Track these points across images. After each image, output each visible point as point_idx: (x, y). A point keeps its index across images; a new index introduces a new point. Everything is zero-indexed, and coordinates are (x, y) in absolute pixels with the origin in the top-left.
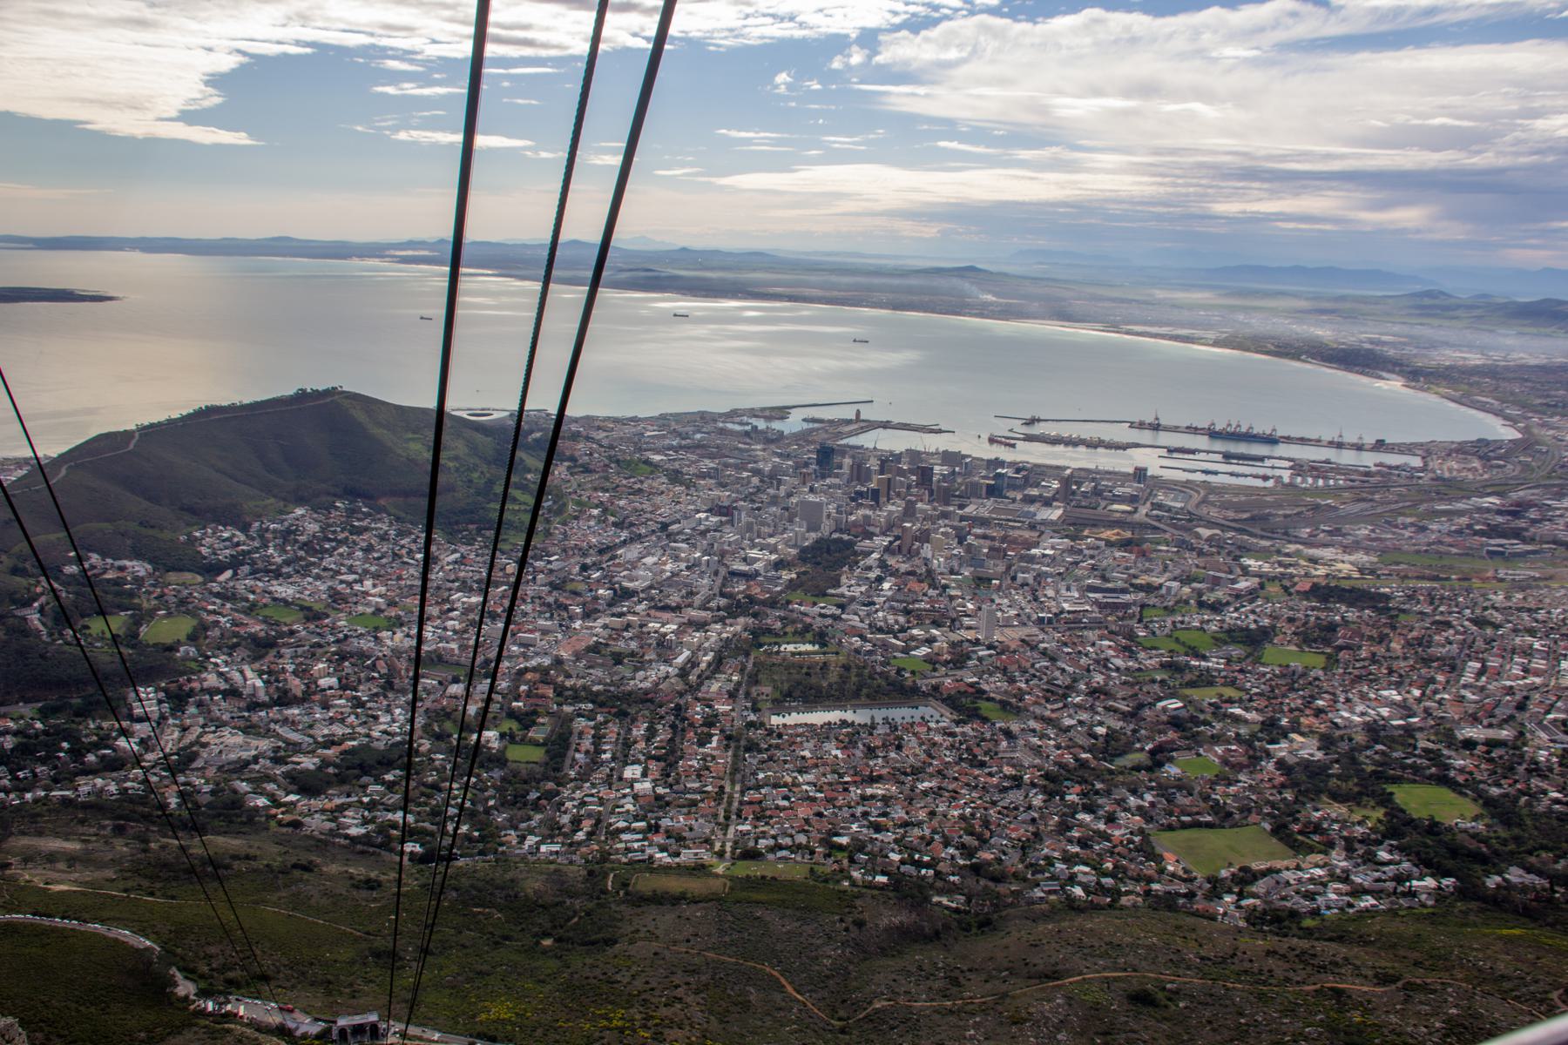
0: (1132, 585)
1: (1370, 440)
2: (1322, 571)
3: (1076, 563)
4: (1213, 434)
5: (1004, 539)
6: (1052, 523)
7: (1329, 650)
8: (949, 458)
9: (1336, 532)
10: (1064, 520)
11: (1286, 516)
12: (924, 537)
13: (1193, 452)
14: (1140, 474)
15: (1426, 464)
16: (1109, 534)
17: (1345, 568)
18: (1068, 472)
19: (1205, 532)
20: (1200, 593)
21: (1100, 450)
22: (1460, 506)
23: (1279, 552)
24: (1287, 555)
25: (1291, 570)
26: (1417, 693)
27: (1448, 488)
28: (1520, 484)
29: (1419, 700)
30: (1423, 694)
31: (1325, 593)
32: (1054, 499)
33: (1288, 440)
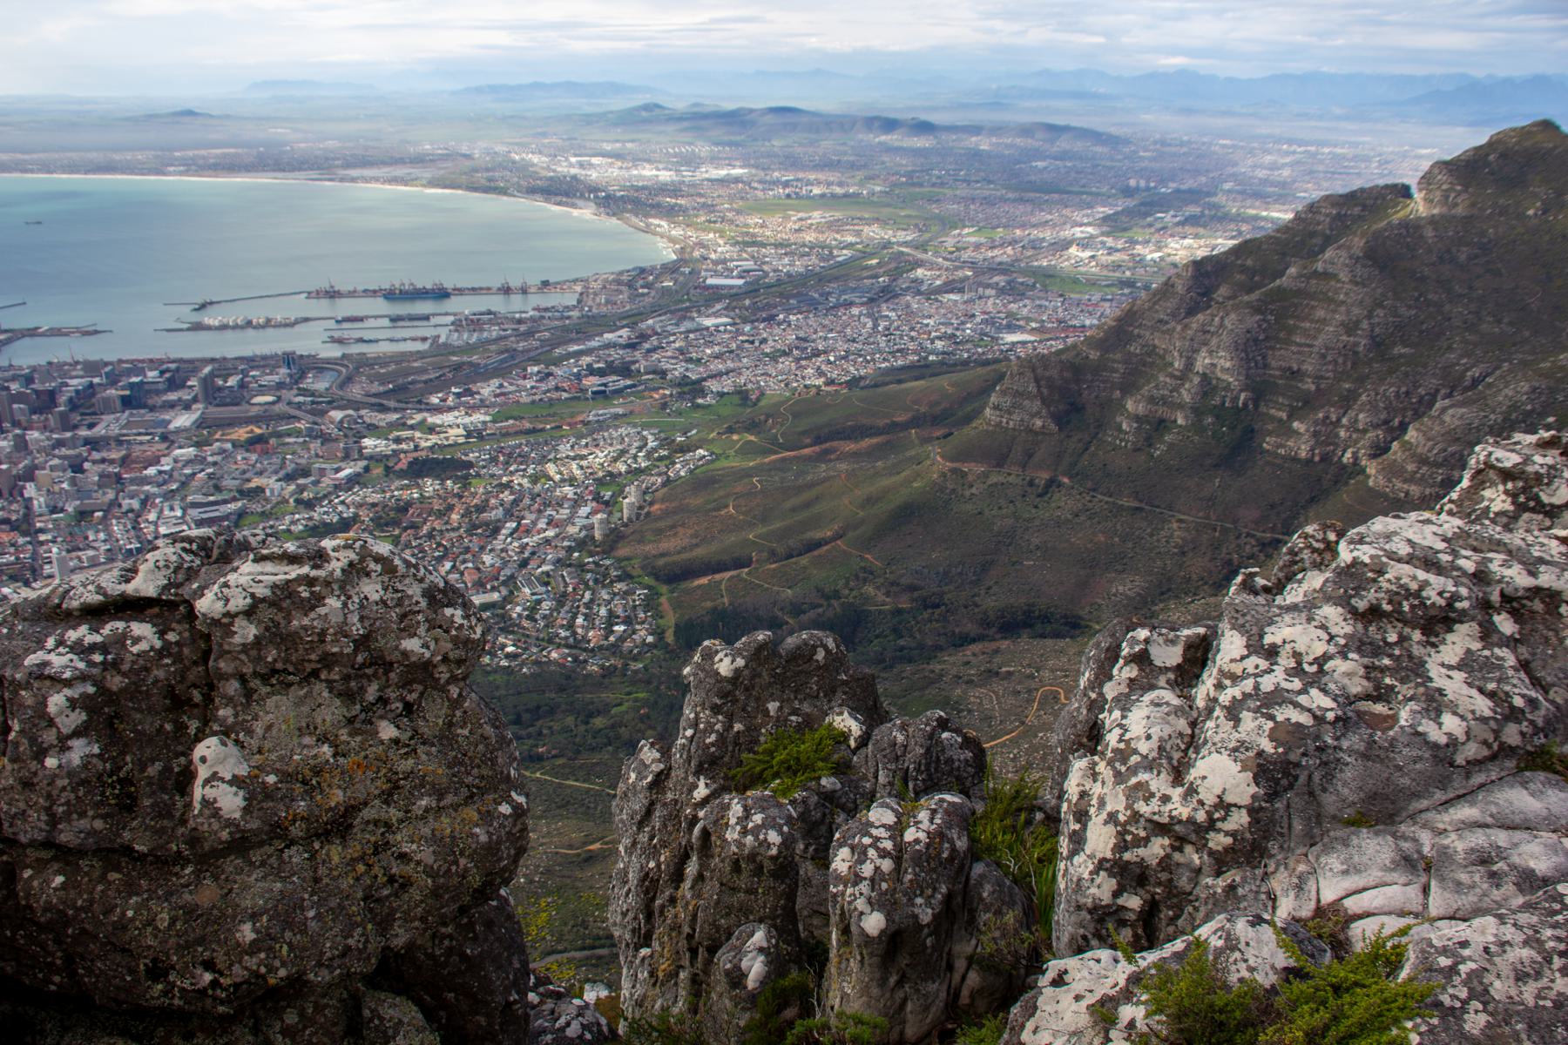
0: (241, 492)
1: (534, 280)
2: (434, 439)
3: (194, 474)
4: (390, 295)
5: (124, 462)
6: (186, 430)
7: (397, 532)
8: (92, 368)
9: (469, 393)
10: (201, 424)
11: (426, 382)
12: (29, 475)
13: (361, 319)
14: (289, 359)
15: (579, 301)
16: (242, 433)
17: (456, 435)
18: (207, 370)
19: (337, 415)
20: (301, 489)
21: (270, 331)
22: (594, 344)
23: (404, 426)
24: (412, 427)
25: (404, 446)
26: (448, 565)
27: (590, 325)
28: (654, 310)
29: (448, 573)
30: (454, 567)
31: (421, 468)
32: (195, 400)
33: (460, 291)
